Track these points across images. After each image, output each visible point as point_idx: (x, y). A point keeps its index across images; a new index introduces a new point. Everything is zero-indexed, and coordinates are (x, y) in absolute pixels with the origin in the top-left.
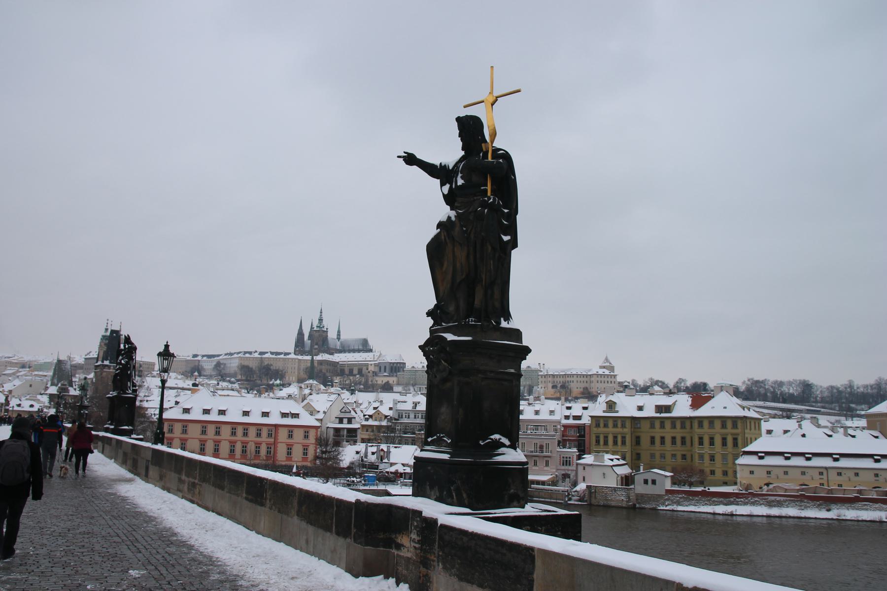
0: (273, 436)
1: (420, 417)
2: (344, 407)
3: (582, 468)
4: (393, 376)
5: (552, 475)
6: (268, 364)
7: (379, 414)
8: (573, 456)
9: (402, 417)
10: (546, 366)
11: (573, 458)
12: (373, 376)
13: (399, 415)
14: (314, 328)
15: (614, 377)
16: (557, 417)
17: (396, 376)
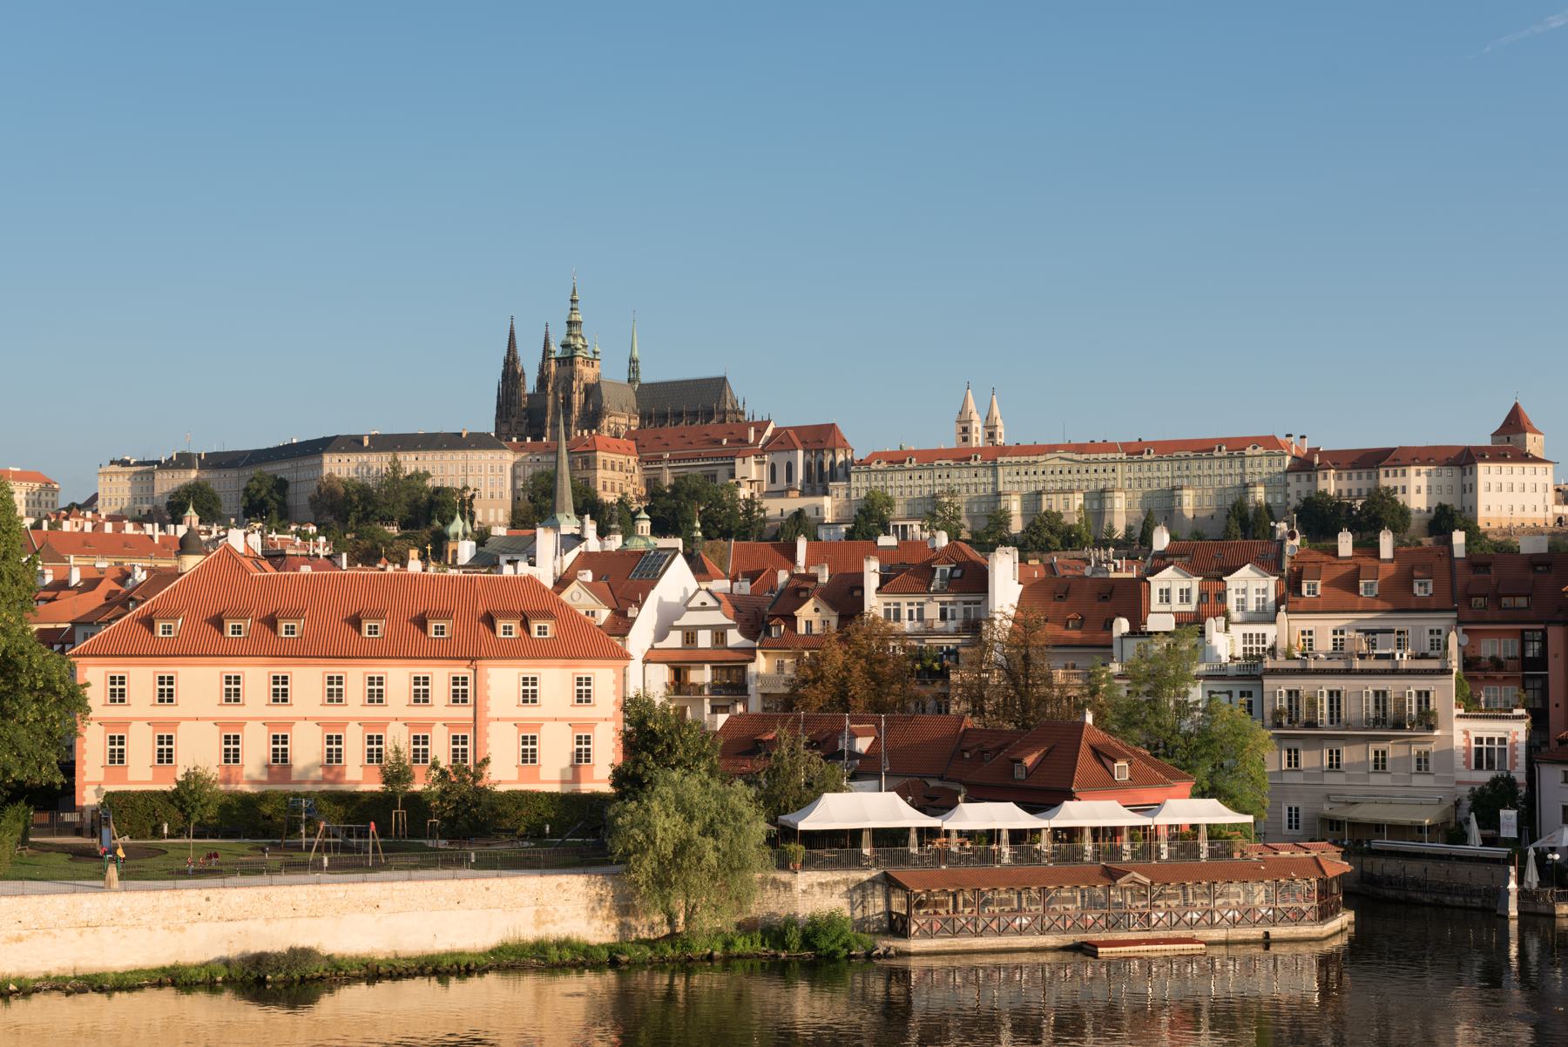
9: (898, 618)
12: (752, 494)
13: (887, 612)
17: (826, 493)
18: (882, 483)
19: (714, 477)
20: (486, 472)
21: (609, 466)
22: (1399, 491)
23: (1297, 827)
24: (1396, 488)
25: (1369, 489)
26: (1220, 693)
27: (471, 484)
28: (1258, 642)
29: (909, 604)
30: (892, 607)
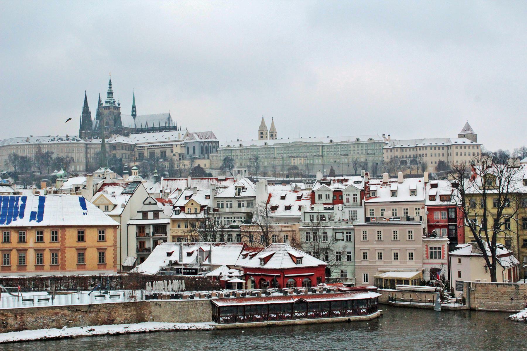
0: (60, 239)
1: (245, 205)
2: (148, 197)
3: (457, 261)
4: (204, 158)
5: (417, 270)
6: (48, 151)
7: (192, 204)
8: (443, 245)
9: (222, 207)
10: (392, 138)
11: (443, 248)
12: (180, 159)
13: (218, 204)
14: (102, 104)
15: (478, 148)
16: (420, 197)
17: (208, 158)
18: (230, 154)
19: (165, 152)
20: (75, 150)
21: (124, 148)
22: (424, 155)
23: (367, 281)
24: (423, 154)
25: (414, 155)
26: (339, 233)
27: (70, 155)
28: (354, 214)
29: (227, 201)
30: (220, 203)
